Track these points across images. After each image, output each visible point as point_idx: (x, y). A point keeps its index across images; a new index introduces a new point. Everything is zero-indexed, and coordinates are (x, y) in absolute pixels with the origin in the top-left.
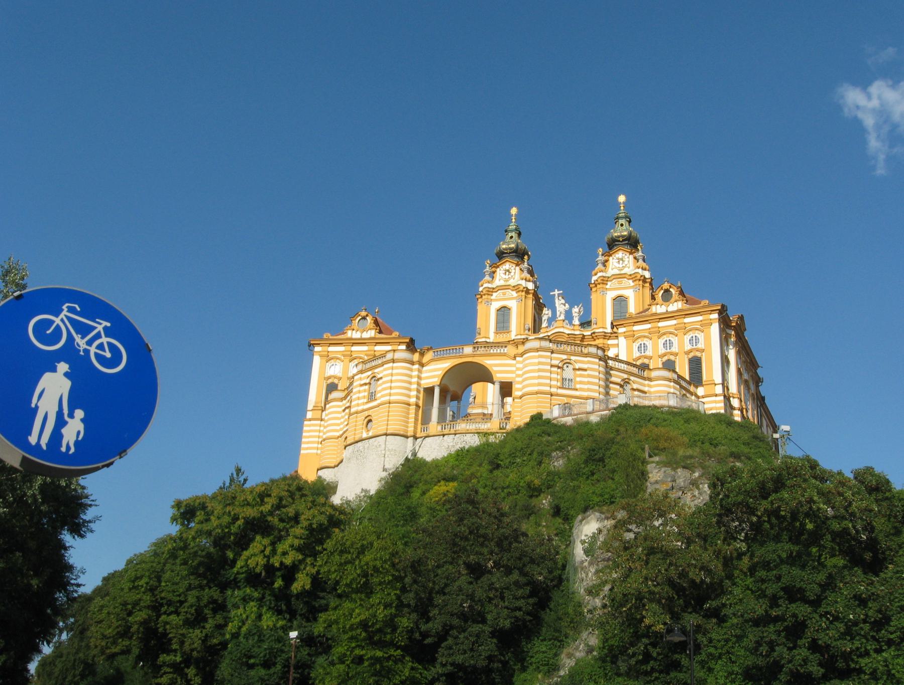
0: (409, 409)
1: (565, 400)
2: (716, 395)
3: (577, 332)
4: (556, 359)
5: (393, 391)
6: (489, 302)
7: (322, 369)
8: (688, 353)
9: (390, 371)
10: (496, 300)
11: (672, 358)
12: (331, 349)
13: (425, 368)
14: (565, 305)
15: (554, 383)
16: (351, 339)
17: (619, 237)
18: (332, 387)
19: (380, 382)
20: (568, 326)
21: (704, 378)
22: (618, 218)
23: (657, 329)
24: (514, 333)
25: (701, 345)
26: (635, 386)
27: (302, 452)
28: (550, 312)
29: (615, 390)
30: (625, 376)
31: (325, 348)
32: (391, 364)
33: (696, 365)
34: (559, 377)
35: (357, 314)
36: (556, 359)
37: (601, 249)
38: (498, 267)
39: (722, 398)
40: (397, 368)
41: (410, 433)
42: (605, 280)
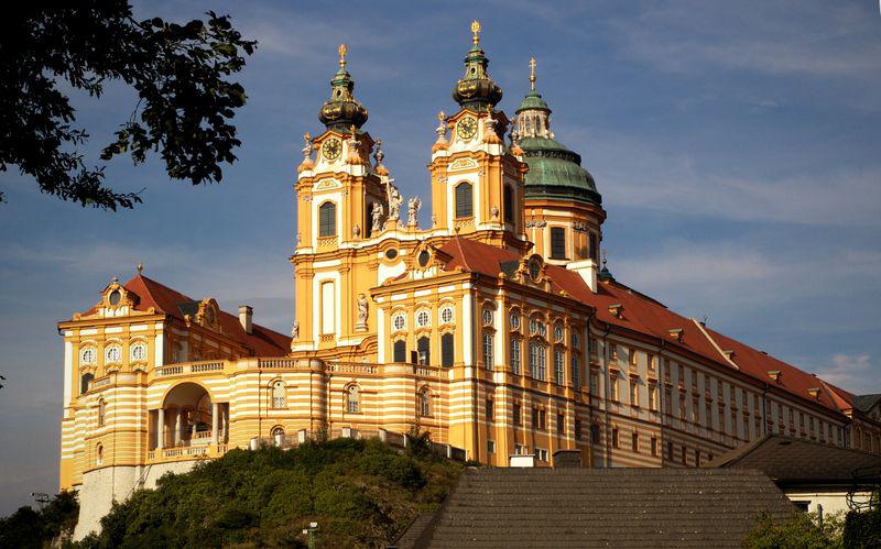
0: (135, 436)
1: (275, 422)
2: (464, 380)
3: (412, 237)
4: (266, 379)
5: (118, 418)
6: (310, 197)
7: (76, 359)
8: (441, 329)
9: (113, 397)
10: (318, 193)
11: (427, 335)
12: (84, 332)
13: (149, 389)
14: (398, 198)
15: (263, 405)
16: (105, 319)
17: (465, 92)
18: (87, 378)
19: (107, 406)
20: (402, 229)
21: (455, 361)
22: (467, 61)
23: (412, 301)
24: (341, 241)
25: (453, 321)
26: (363, 388)
27: (63, 457)
28: (381, 207)
29: (338, 397)
30: (350, 380)
31: (76, 332)
32: (114, 389)
33: (448, 342)
34: (269, 398)
35: (108, 288)
36: (266, 379)
37: (442, 114)
38: (320, 142)
39: (469, 383)
40: (119, 393)
41: (138, 462)
42: (445, 161)
